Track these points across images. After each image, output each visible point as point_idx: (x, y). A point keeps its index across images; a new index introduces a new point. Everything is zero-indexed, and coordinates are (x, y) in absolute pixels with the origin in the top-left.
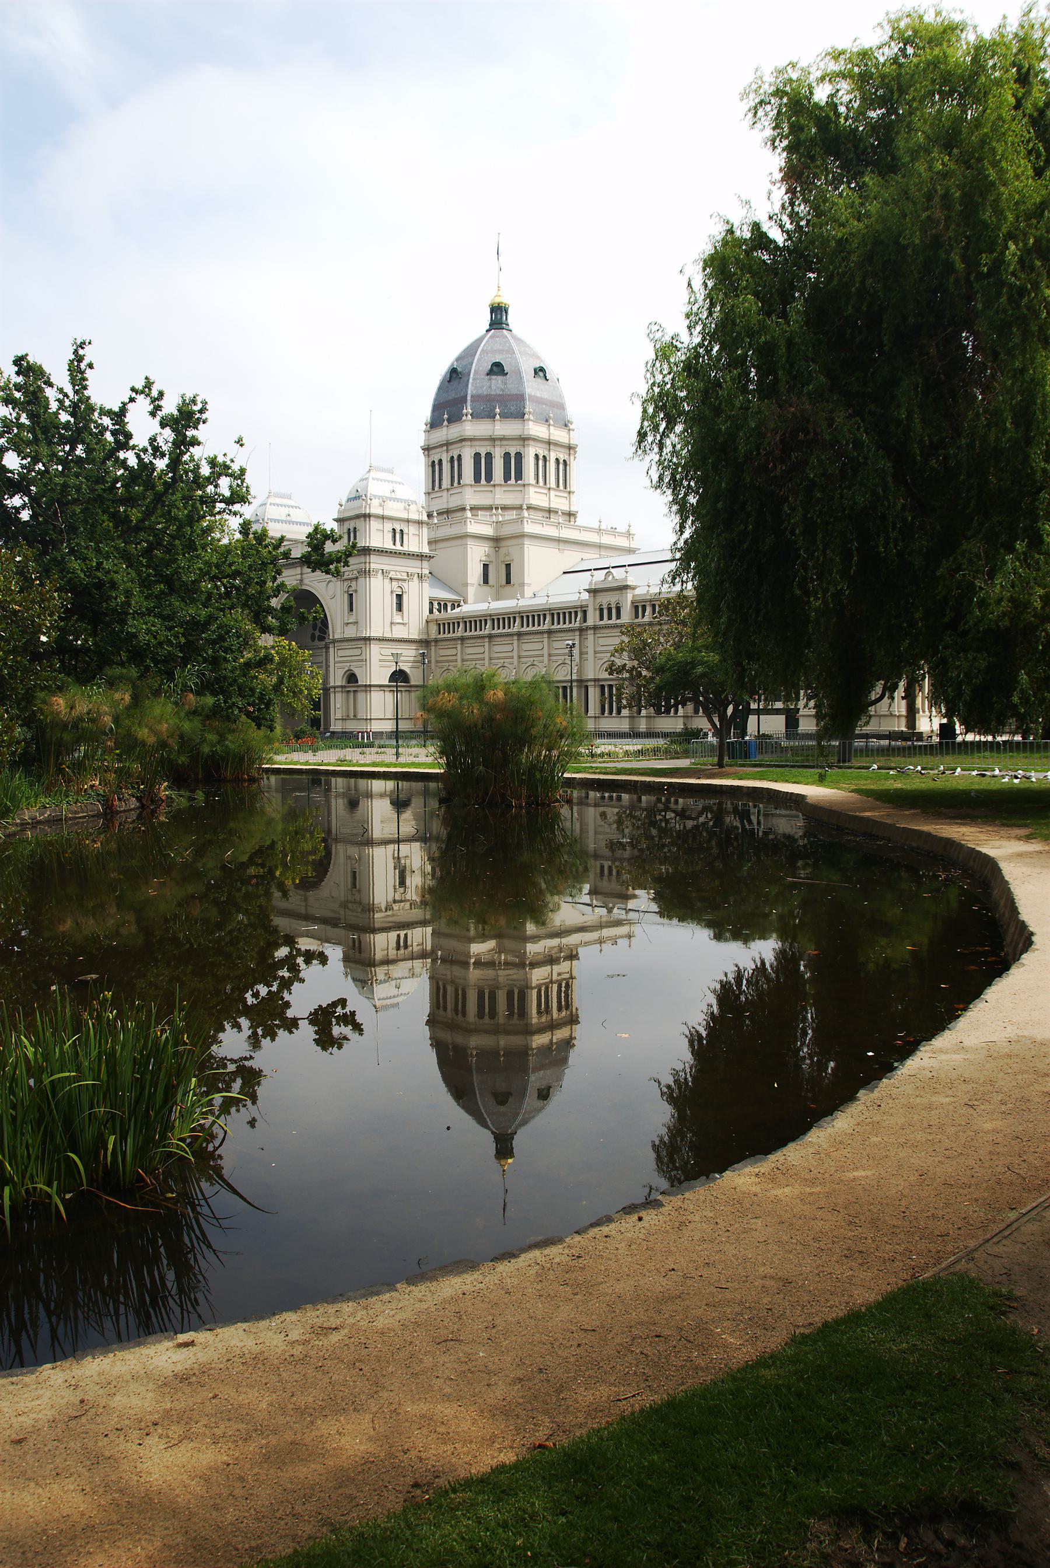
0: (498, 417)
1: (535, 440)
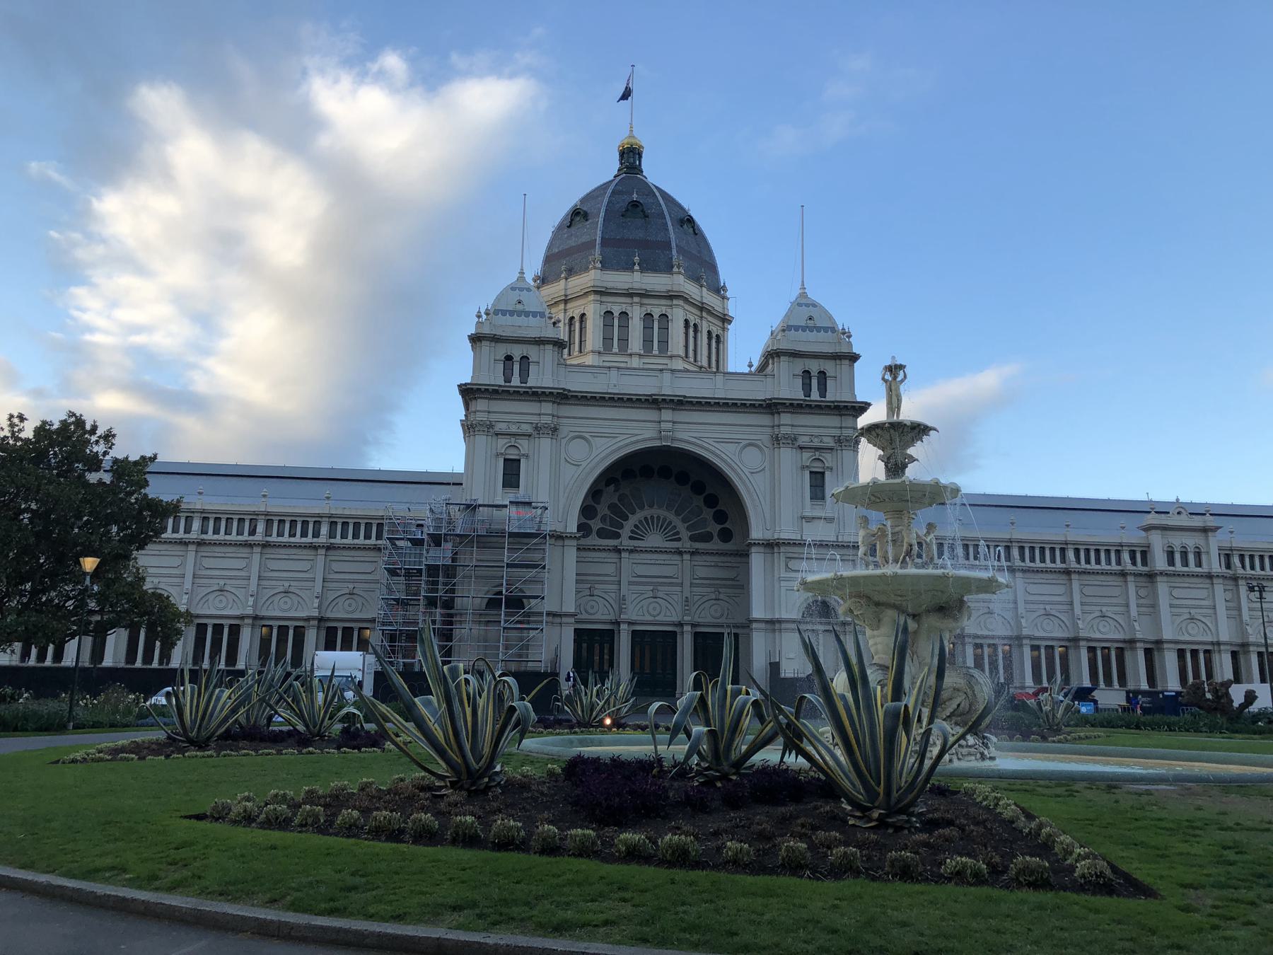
0: (637, 267)
1: (686, 300)
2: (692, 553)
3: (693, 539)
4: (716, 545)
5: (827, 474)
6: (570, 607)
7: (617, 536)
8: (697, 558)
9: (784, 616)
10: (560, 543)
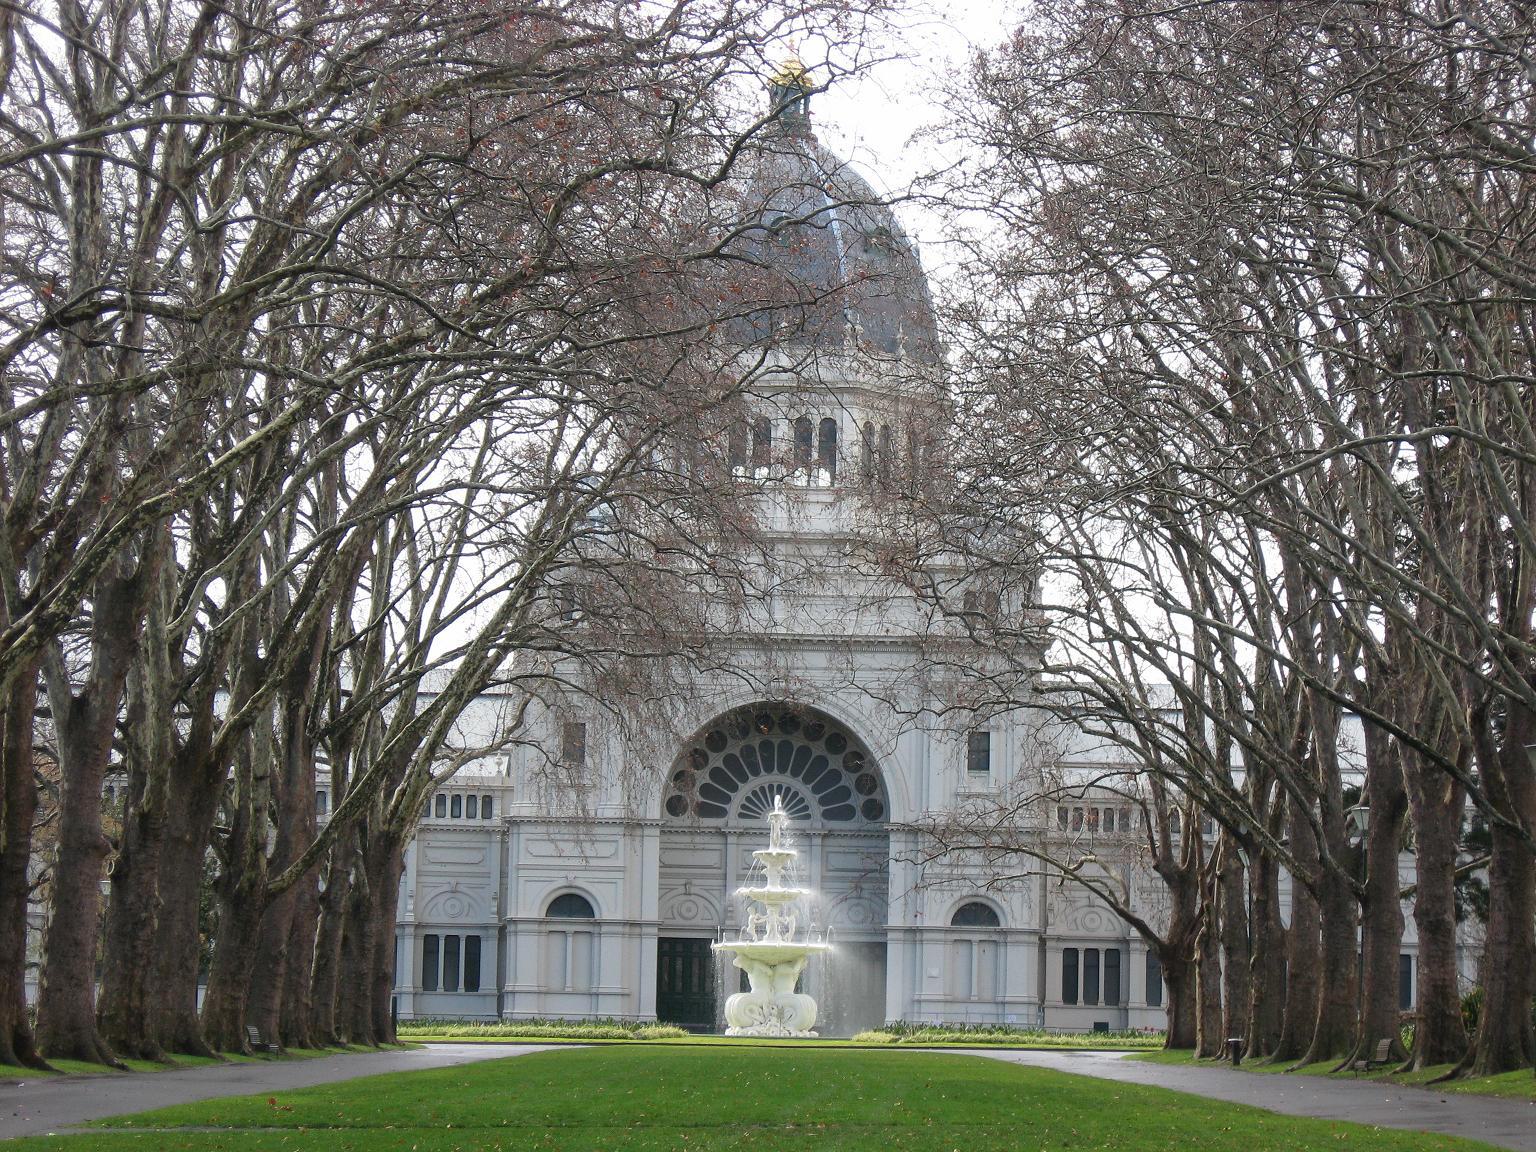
2: (825, 836)
3: (827, 815)
4: (858, 822)
5: (993, 736)
6: (651, 914)
7: (722, 813)
8: (831, 841)
9: (927, 923)
10: (638, 832)
